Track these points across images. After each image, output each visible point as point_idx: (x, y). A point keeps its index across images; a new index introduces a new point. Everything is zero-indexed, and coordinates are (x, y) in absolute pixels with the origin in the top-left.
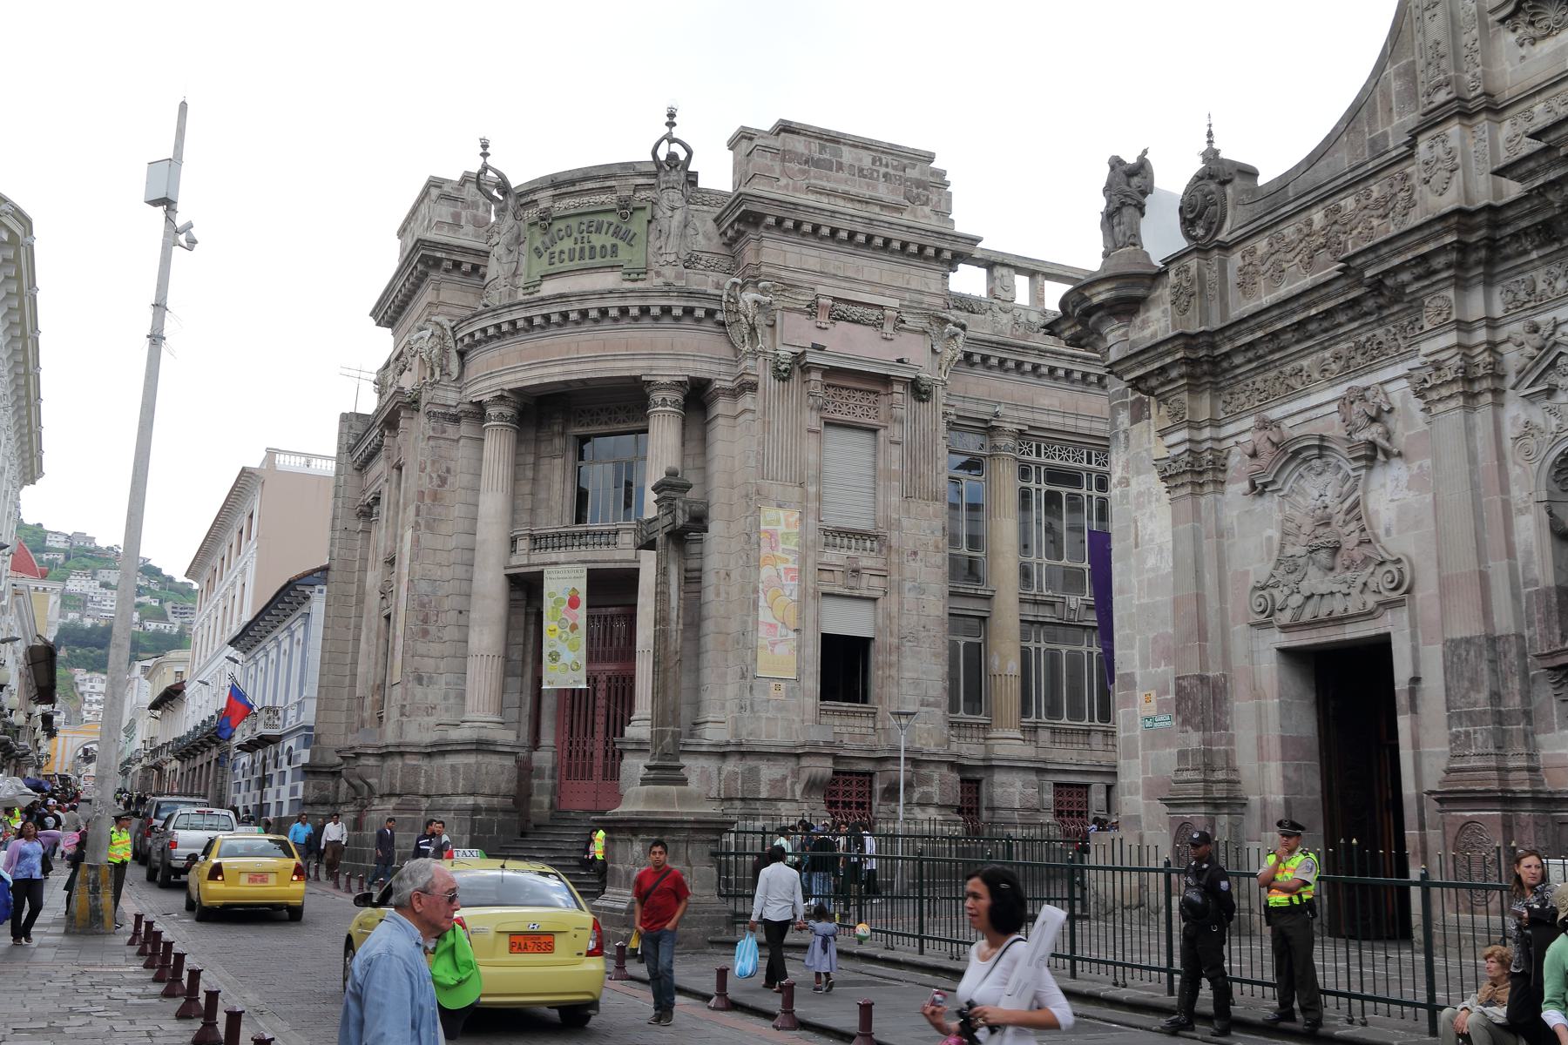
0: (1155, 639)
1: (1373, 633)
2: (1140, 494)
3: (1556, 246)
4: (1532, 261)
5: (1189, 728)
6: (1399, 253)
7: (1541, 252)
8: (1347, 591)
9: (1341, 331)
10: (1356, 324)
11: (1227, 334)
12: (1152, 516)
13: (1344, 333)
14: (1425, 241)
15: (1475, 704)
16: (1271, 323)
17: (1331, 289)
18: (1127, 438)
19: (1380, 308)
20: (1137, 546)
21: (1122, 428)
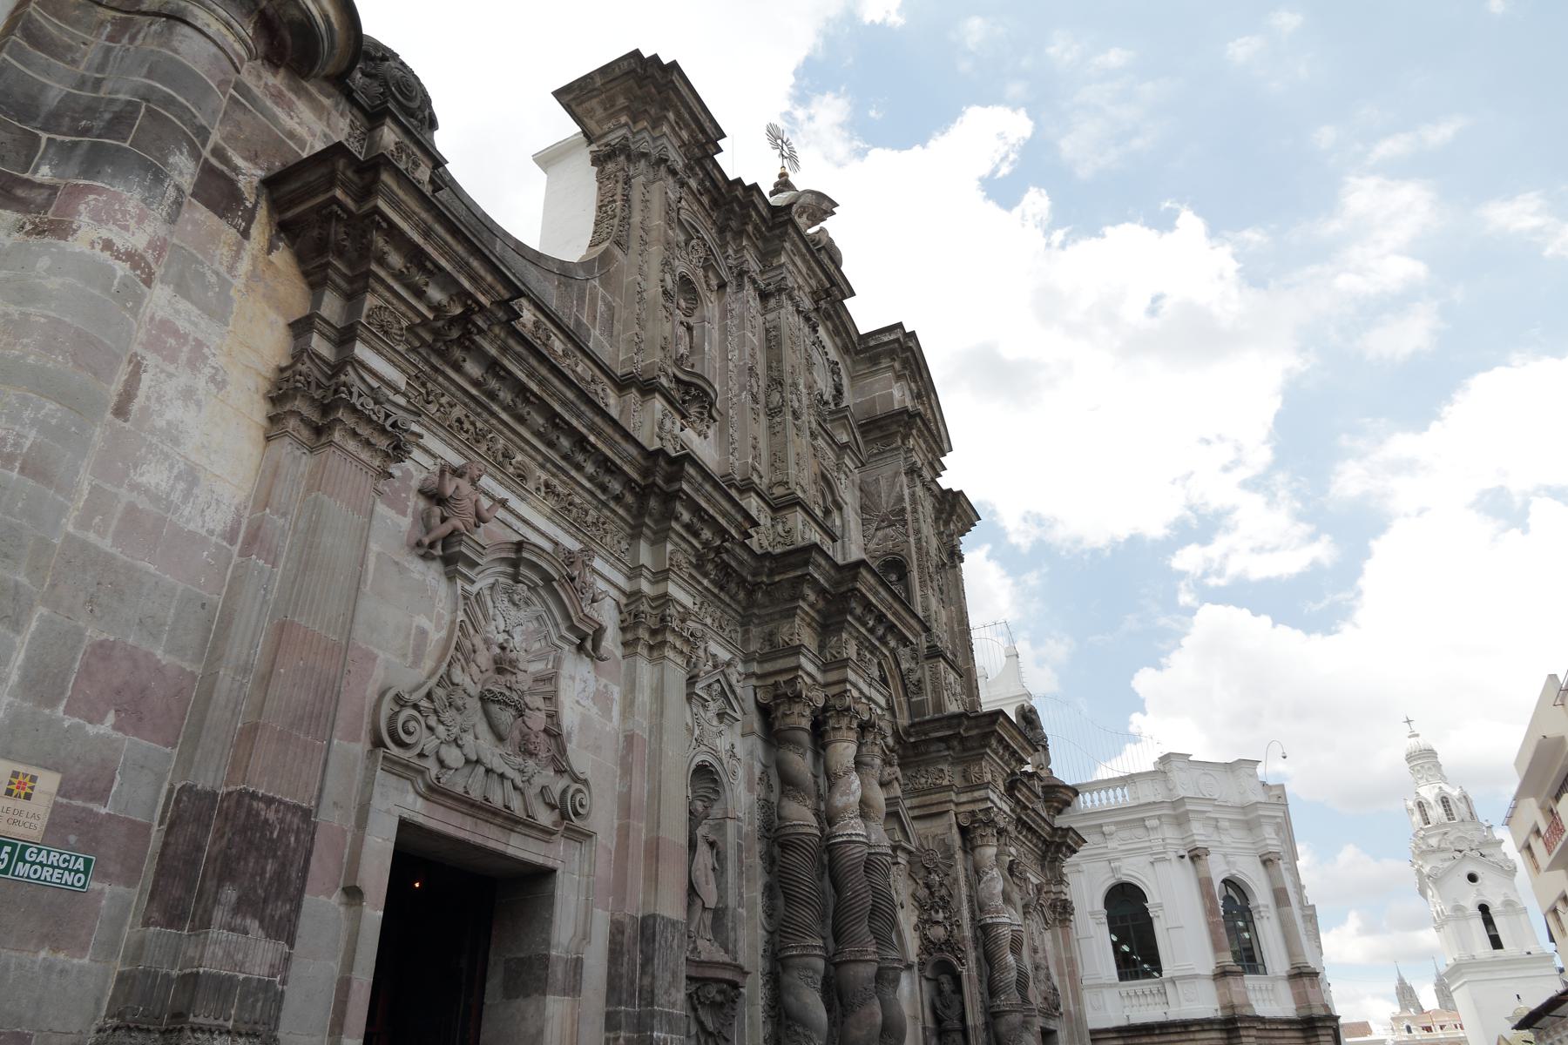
0: (103, 651)
1: (540, 860)
2: (166, 327)
3: (716, 591)
4: (700, 583)
5: (253, 925)
6: (708, 501)
7: (711, 587)
8: (521, 785)
9: (573, 473)
10: (588, 485)
11: (511, 342)
12: (188, 394)
13: (572, 478)
14: (725, 514)
15: (674, 1005)
16: (552, 395)
17: (624, 444)
18: (178, 204)
19: (618, 499)
20: (121, 411)
21: (178, 179)
